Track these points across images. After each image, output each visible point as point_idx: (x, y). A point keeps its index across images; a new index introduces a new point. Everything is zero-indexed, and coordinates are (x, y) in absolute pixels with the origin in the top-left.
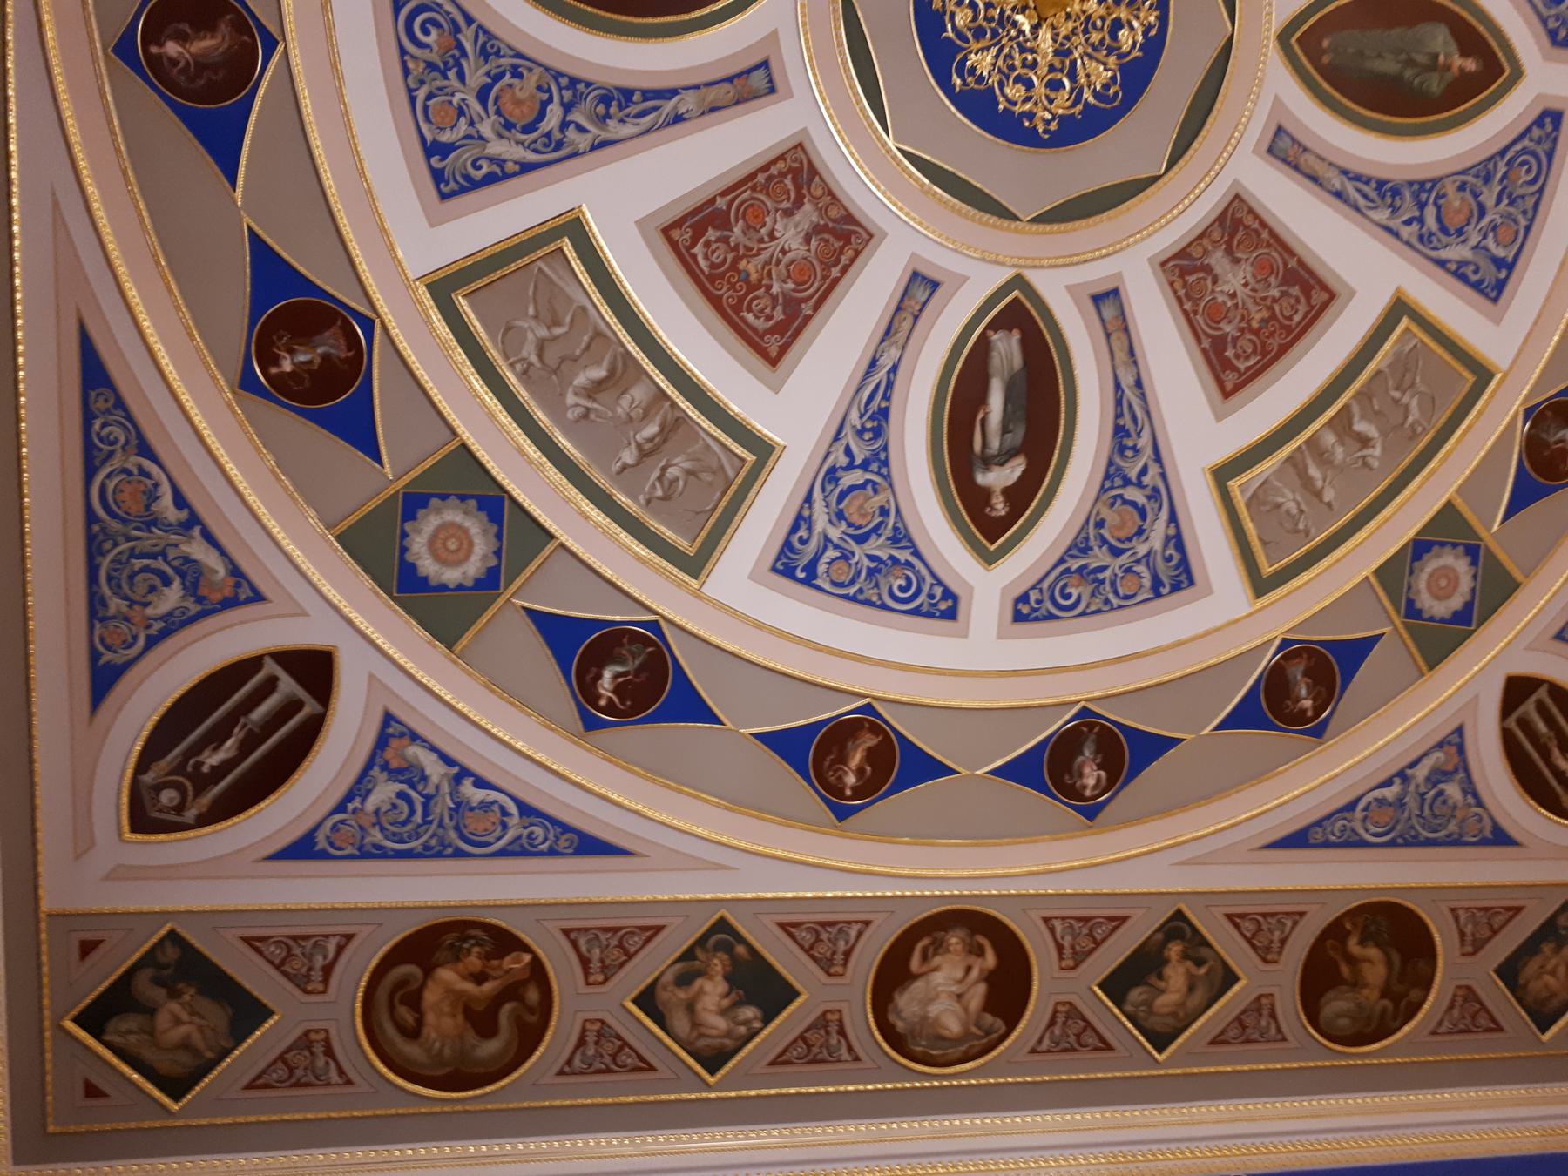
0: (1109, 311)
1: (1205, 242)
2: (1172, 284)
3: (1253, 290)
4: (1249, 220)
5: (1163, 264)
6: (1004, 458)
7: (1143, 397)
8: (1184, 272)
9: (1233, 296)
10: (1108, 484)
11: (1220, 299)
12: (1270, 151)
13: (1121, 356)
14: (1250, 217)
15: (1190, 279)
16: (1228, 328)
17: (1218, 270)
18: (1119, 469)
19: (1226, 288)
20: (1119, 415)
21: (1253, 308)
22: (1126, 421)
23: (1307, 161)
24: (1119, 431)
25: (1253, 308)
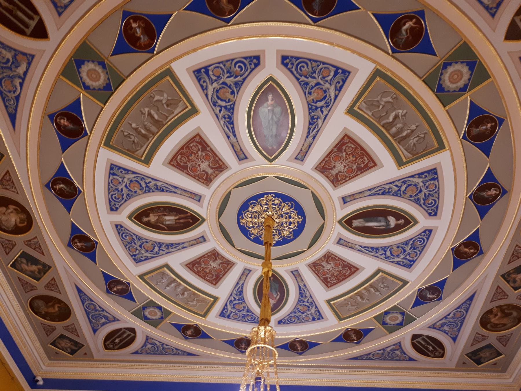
0: (348, 199)
1: (329, 176)
2: (341, 184)
3: (343, 160)
4: (323, 164)
5: (335, 187)
6: (387, 221)
7: (374, 188)
8: (338, 181)
9: (345, 166)
10: (399, 195)
11: (346, 170)
12: (302, 161)
13: (361, 195)
14: (322, 164)
15: (340, 179)
16: (355, 167)
17: (337, 171)
18: (395, 193)
19: (343, 169)
20: (379, 194)
21: (349, 160)
22: (380, 192)
23: (304, 150)
24: (383, 194)
25: (349, 160)
